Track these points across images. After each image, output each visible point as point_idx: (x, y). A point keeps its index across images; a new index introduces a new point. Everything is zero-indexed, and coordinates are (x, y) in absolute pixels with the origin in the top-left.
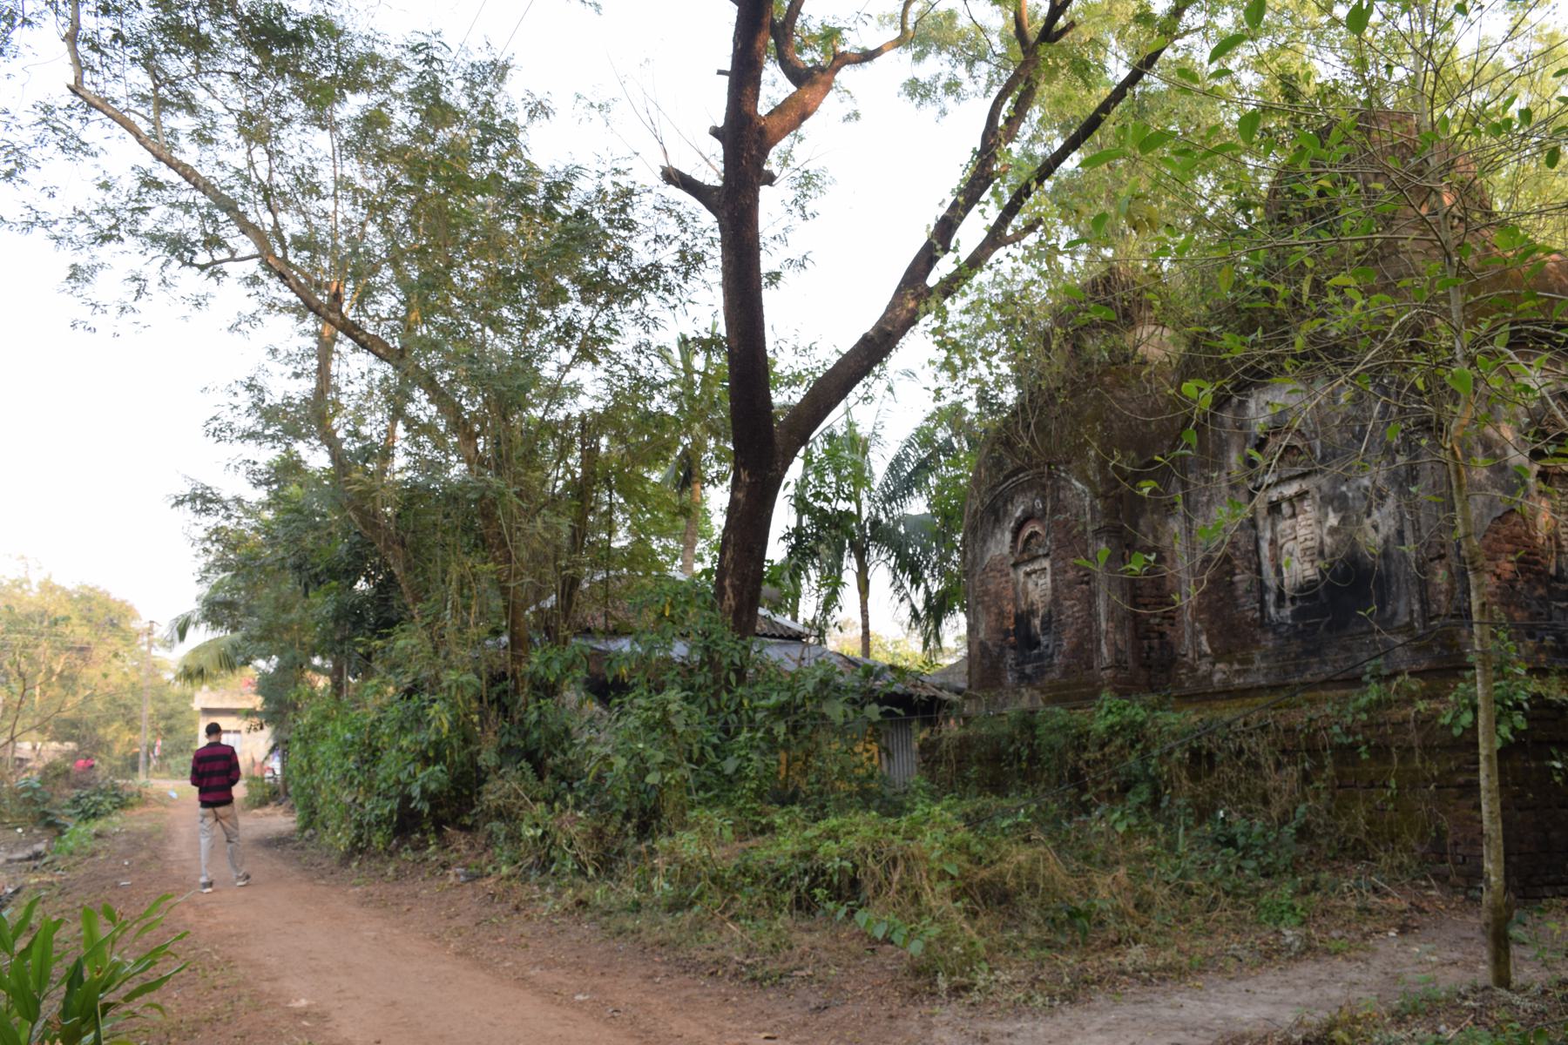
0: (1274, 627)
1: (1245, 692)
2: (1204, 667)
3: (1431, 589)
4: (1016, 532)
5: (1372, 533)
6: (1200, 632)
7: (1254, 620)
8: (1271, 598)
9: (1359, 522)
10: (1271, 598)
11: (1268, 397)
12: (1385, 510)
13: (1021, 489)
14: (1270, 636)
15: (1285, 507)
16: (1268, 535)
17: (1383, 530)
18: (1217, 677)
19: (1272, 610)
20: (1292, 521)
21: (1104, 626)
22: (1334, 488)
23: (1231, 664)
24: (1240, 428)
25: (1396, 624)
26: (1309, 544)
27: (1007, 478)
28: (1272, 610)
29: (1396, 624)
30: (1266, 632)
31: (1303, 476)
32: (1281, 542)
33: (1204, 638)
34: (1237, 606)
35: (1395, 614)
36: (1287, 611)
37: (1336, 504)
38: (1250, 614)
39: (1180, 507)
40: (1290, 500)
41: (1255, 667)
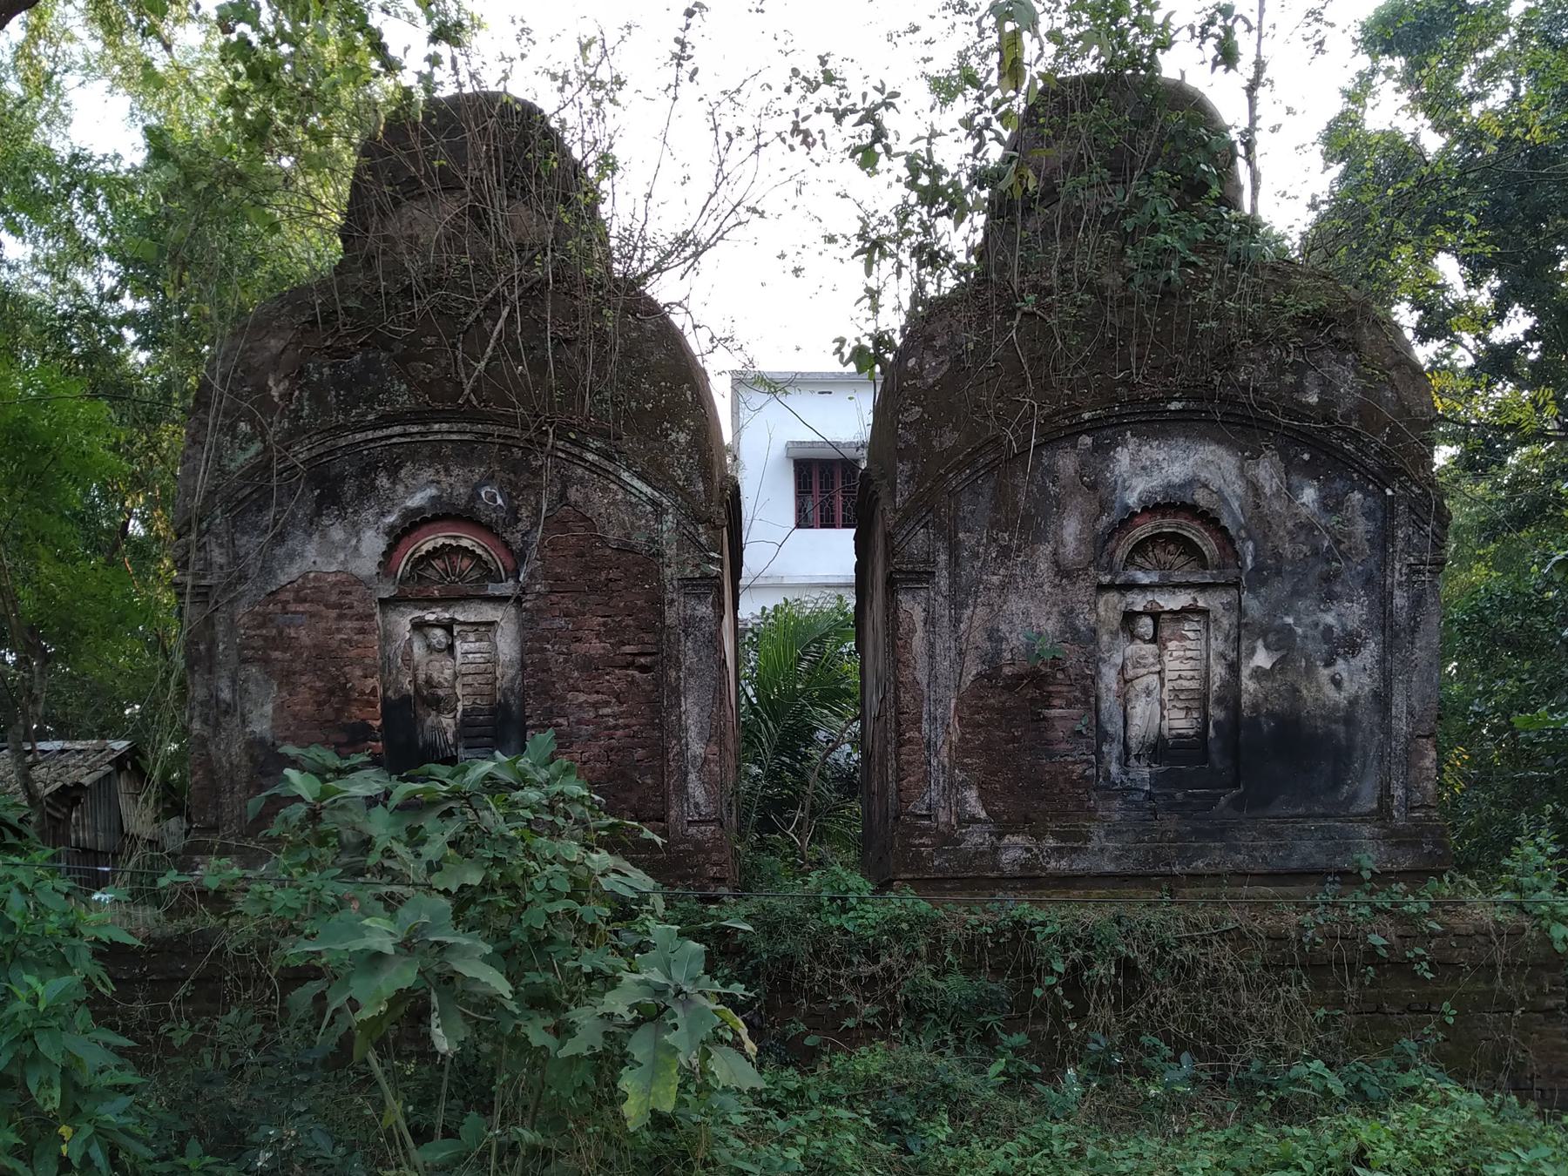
4: (398, 537)
5: (1330, 690)
6: (965, 784)
8: (1112, 750)
9: (1310, 671)
11: (1161, 456)
12: (1357, 662)
14: (1117, 803)
17: (1350, 688)
19: (1114, 768)
21: (697, 748)
22: (1272, 614)
23: (1039, 837)
25: (1354, 809)
28: (1114, 768)
29: (1354, 809)
31: (1202, 587)
33: (972, 795)
34: (1051, 756)
35: (1353, 797)
36: (1143, 772)
37: (1271, 638)
38: (1079, 769)
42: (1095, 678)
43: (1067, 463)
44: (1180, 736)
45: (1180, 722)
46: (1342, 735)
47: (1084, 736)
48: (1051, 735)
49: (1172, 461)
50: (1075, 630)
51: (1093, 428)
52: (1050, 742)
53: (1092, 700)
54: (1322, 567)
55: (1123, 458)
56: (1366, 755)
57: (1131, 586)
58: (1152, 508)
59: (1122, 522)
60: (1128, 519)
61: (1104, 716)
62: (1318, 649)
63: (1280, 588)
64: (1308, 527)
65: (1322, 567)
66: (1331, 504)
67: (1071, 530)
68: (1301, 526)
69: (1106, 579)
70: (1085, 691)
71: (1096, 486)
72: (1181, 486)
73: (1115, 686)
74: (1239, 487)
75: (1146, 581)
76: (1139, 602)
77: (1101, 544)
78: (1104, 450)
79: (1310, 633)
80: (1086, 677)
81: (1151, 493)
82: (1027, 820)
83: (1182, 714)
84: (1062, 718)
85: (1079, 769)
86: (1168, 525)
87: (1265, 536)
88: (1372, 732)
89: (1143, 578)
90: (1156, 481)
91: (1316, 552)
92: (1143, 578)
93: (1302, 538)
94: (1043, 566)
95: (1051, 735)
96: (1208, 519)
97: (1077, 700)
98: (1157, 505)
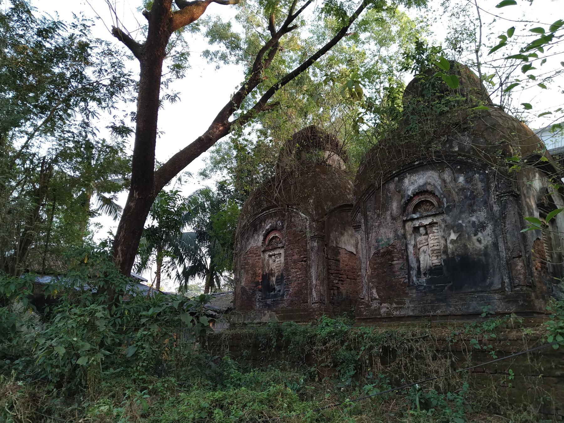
0: (417, 287)
1: (399, 318)
2: (375, 305)
3: (514, 272)
7: (405, 283)
8: (414, 273)
10: (414, 273)
11: (416, 178)
13: (270, 216)
15: (422, 230)
16: (413, 242)
18: (383, 311)
19: (415, 279)
20: (426, 237)
24: (399, 192)
26: (436, 248)
27: (263, 211)
28: (415, 279)
30: (412, 289)
32: (419, 246)
36: (423, 279)
38: (402, 280)
39: (363, 227)
40: (425, 227)
41: (406, 306)
42: (406, 249)
43: (392, 186)
44: (436, 266)
45: (435, 261)
46: (484, 260)
47: (403, 269)
48: (394, 270)
49: (420, 179)
50: (398, 236)
51: (397, 175)
52: (394, 272)
53: (405, 257)
54: (469, 202)
55: (406, 181)
56: (494, 267)
57: (412, 220)
58: (416, 194)
59: (408, 200)
60: (411, 199)
61: (410, 261)
62: (471, 230)
63: (456, 211)
64: (463, 189)
65: (469, 202)
66: (469, 180)
67: (395, 205)
68: (460, 190)
69: (405, 218)
70: (402, 254)
71: (400, 191)
72: (423, 186)
73: (412, 252)
74: (439, 182)
75: (416, 217)
76: (417, 223)
77: (404, 209)
78: (401, 180)
79: (468, 225)
80: (402, 250)
81: (414, 190)
82: (390, 298)
83: (436, 258)
84: (397, 264)
85: (402, 280)
86: (423, 198)
87: (449, 195)
88: (495, 258)
89: (415, 216)
90: (416, 186)
91: (466, 197)
92: (415, 216)
93: (461, 193)
94: (388, 218)
95: (394, 270)
96: (432, 193)
97: (400, 258)
98: (417, 193)
